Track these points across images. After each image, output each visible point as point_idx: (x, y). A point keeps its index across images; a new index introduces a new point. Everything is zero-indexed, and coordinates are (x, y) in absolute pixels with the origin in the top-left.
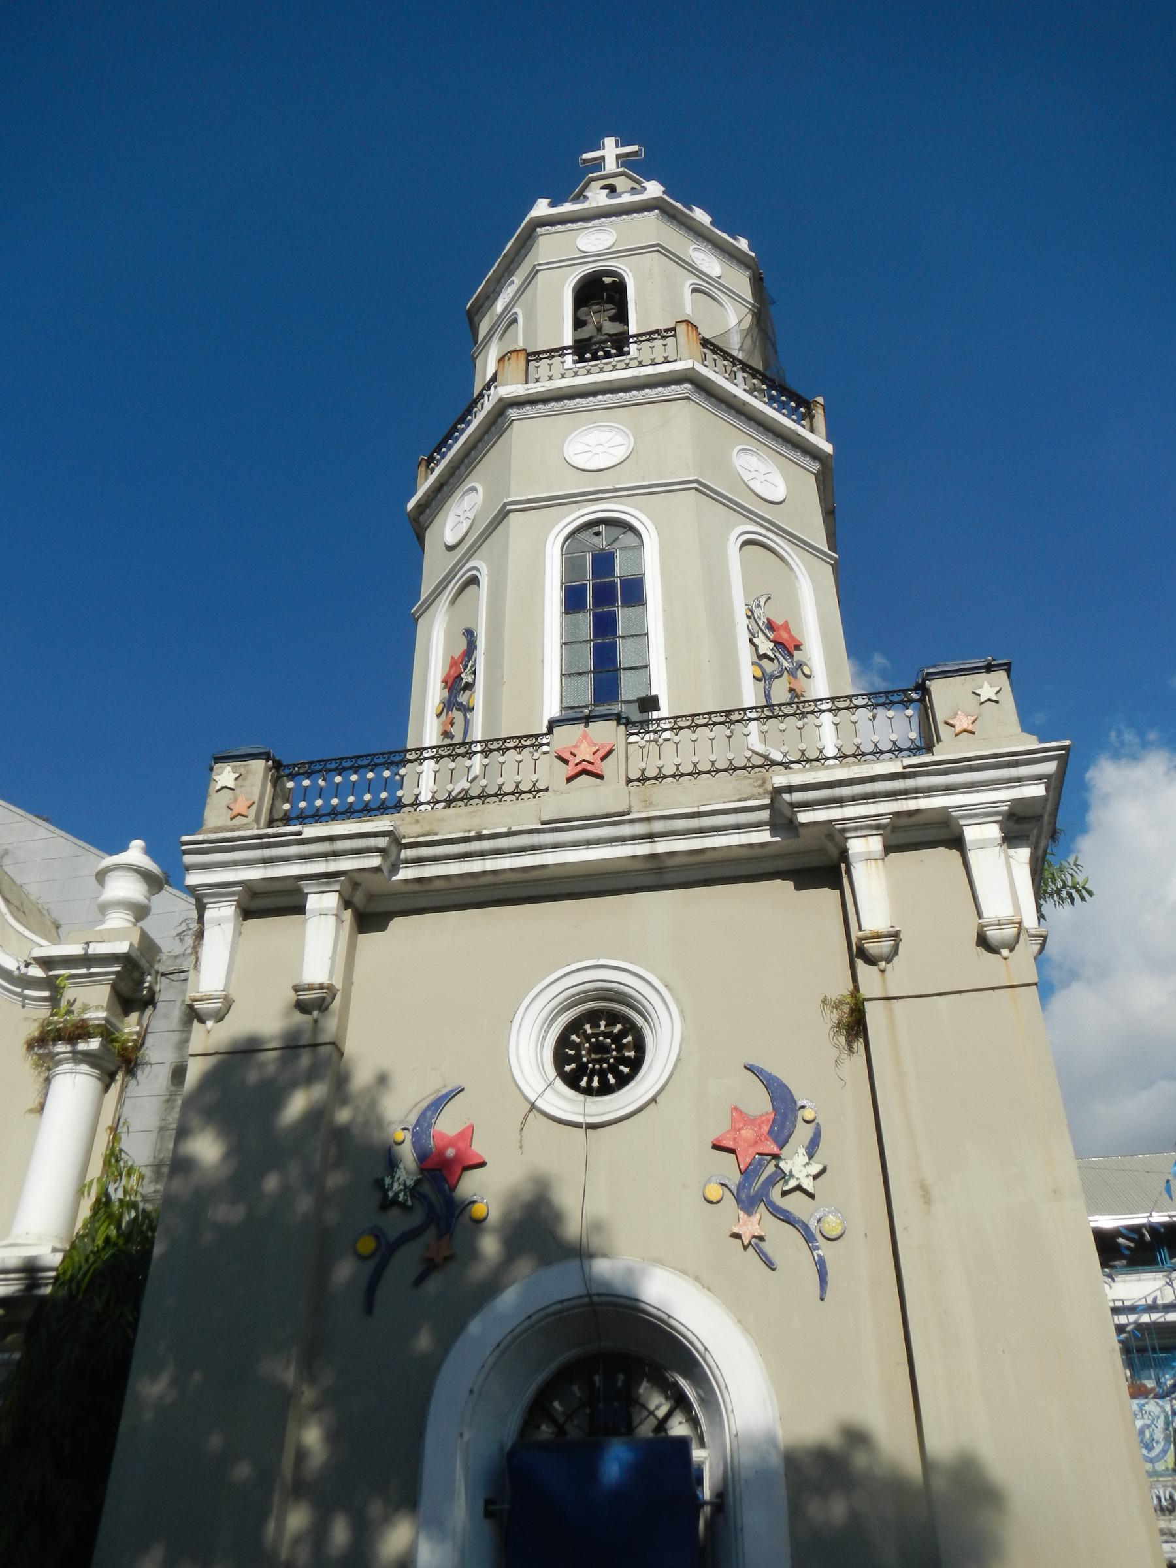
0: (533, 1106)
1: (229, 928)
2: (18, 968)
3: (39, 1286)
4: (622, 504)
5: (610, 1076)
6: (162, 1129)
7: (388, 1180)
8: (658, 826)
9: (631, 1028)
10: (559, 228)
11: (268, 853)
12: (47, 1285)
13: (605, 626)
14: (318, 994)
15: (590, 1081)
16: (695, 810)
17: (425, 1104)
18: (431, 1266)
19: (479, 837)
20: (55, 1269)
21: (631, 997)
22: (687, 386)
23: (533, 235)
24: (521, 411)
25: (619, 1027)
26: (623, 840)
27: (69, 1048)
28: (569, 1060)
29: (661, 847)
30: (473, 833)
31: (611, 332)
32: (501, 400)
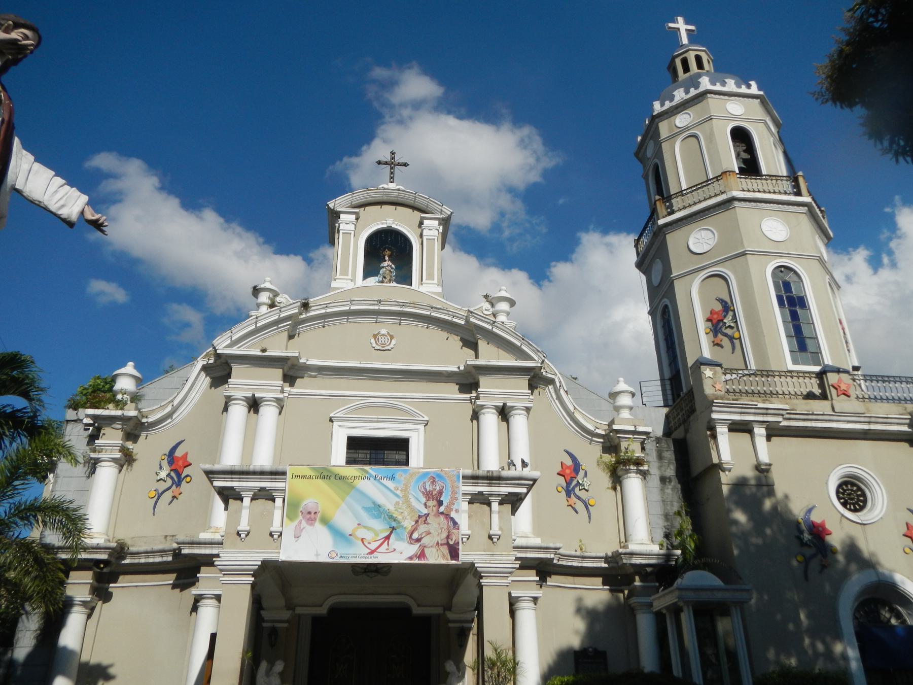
0: (843, 515)
1: (726, 436)
2: (595, 430)
3: (670, 561)
4: (791, 260)
5: (856, 506)
6: (663, 501)
7: (802, 536)
8: (873, 420)
9: (859, 489)
10: (717, 96)
11: (743, 410)
12: (673, 561)
13: (794, 316)
14: (767, 467)
15: (850, 507)
16: (886, 416)
17: (805, 510)
18: (824, 567)
19: (813, 414)
20: (678, 556)
21: (863, 479)
22: (806, 208)
23: (705, 96)
24: (740, 203)
25: (855, 488)
26: (860, 422)
27: (635, 468)
28: (842, 498)
29: (873, 427)
30: (811, 413)
31: (744, 157)
32: (733, 197)
